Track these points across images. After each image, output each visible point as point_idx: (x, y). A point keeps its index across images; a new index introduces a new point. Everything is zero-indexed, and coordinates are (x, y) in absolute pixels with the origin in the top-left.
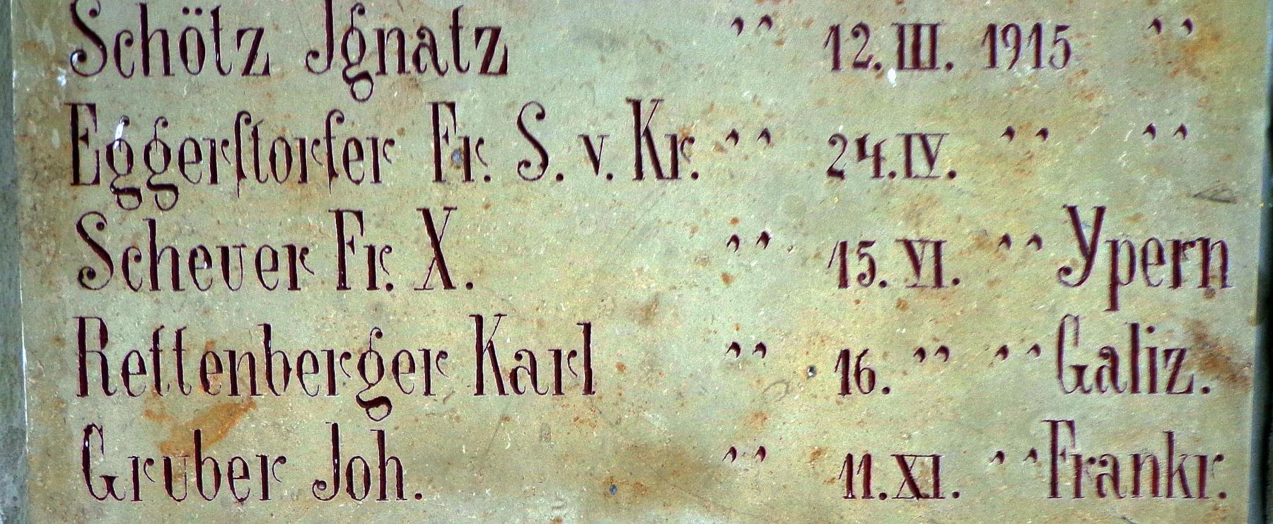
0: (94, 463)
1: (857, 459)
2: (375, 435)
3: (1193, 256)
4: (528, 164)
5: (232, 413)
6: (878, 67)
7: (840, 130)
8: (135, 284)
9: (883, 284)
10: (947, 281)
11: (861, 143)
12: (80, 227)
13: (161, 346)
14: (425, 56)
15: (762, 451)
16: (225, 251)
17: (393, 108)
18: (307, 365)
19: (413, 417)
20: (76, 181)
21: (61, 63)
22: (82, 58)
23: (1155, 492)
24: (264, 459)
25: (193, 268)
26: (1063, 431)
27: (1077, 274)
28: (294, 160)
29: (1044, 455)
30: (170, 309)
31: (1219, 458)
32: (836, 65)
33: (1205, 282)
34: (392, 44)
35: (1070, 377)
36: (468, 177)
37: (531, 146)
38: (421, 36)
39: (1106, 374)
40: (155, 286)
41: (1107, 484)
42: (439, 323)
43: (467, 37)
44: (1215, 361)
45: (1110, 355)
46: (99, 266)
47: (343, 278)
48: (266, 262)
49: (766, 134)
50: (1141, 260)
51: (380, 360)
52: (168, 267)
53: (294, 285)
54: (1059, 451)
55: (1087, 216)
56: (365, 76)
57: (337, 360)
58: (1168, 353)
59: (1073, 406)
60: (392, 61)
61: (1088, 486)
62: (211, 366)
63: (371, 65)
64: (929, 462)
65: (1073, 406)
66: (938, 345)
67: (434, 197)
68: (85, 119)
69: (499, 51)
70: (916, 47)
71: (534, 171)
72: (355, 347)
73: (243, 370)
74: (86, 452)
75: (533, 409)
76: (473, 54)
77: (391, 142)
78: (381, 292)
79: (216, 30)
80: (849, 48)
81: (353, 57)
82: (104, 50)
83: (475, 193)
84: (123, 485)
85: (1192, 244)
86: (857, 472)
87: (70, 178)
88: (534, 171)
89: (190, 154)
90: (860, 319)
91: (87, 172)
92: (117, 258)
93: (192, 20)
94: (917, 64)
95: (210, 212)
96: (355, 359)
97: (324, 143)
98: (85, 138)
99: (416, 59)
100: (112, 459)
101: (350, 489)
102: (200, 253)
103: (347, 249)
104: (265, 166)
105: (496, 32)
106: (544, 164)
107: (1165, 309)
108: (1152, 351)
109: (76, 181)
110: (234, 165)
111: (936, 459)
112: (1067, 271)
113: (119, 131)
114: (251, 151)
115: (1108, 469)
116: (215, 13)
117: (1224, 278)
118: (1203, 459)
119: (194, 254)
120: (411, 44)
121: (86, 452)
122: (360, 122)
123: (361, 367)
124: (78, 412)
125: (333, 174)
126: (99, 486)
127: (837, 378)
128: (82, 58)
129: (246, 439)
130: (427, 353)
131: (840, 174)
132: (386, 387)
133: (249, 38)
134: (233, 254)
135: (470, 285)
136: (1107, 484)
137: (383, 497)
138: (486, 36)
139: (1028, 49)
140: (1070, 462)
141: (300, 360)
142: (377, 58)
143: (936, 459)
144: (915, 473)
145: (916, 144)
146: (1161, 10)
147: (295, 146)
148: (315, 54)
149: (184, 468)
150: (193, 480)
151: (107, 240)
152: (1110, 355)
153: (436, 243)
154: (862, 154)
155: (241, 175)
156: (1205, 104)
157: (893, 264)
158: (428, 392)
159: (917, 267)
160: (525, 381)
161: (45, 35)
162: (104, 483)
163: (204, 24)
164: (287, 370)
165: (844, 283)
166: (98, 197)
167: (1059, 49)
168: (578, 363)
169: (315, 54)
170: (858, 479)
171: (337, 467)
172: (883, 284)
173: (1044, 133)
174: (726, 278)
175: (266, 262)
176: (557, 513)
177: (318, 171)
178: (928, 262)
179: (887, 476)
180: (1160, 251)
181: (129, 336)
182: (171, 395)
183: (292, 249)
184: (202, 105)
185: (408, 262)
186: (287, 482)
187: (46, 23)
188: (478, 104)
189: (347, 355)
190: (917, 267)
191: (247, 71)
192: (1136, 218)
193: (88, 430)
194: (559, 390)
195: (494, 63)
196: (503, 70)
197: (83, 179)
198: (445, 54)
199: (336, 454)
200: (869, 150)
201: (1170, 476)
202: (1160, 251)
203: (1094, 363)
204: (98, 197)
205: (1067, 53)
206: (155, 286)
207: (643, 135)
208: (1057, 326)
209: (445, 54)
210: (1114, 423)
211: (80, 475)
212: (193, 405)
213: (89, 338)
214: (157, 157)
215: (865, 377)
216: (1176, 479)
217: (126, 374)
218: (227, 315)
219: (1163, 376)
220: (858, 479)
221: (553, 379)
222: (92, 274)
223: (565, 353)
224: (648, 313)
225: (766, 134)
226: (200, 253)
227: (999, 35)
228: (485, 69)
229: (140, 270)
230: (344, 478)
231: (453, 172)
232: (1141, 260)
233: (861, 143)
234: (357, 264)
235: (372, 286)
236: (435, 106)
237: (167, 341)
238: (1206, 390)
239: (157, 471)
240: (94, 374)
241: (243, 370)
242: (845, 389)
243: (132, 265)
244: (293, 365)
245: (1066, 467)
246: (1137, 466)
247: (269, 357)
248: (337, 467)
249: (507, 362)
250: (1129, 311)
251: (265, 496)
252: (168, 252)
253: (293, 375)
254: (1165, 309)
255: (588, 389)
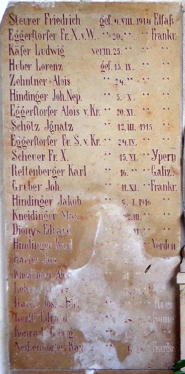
0: (14, 185)
1: (124, 185)
2: (55, 182)
3: (171, 156)
4: (76, 143)
5: (34, 178)
6: (125, 130)
7: (120, 139)
8: (20, 160)
9: (127, 160)
10: (136, 160)
11: (123, 140)
12: (13, 152)
13: (24, 169)
14: (61, 128)
15: (110, 184)
16: (33, 155)
17: (57, 135)
18: (45, 172)
19: (60, 180)
20: (12, 145)
21: (10, 129)
22: (13, 128)
23: (167, 190)
24: (39, 185)
25: (28, 158)
26: (153, 181)
27: (154, 159)
28: (43, 142)
29: (151, 185)
30: (25, 163)
31: (176, 185)
32: (119, 130)
33: (172, 160)
34: (57, 126)
35: (154, 174)
36: (68, 145)
37: (76, 141)
38: (61, 125)
39: (159, 173)
40: (23, 160)
41: (160, 189)
42: (63, 165)
43: (67, 126)
44: (175, 172)
45: (159, 170)
46: (15, 157)
47: (50, 159)
48: (39, 157)
49: (110, 139)
50: (163, 157)
51: (55, 171)
52: (24, 157)
53: (43, 160)
54: (153, 184)
55: (155, 151)
56: (53, 131)
57: (49, 171)
58: (168, 170)
59: (154, 178)
60: (57, 129)
61: (157, 189)
62: (31, 172)
63: (54, 129)
64: (134, 186)
65: (154, 178)
66: (135, 169)
67: (63, 148)
68: (13, 137)
69: (72, 127)
70: (130, 127)
71: (77, 144)
72: (52, 169)
73: (35, 172)
74: (13, 184)
75: (77, 178)
76: (68, 128)
77: (57, 140)
78: (55, 161)
79: (32, 124)
80: (121, 127)
81: (51, 128)
82: (16, 127)
83: (69, 147)
84: (18, 189)
85: (170, 155)
86: (124, 187)
87: (11, 145)
88: (77, 144)
89: (28, 142)
90: (124, 165)
91: (14, 144)
92: (18, 156)
93: (29, 123)
94: (131, 130)
95: (30, 150)
96: (52, 171)
97: (47, 140)
98: (14, 139)
99: (60, 129)
100: (17, 185)
101: (51, 189)
102: (29, 155)
103: (51, 155)
104: (39, 143)
105: (71, 125)
106: (78, 143)
107: (167, 164)
108: (165, 170)
109: (12, 145)
110: (34, 143)
111: (135, 185)
112: (153, 159)
113: (18, 138)
114: (37, 141)
115: (160, 187)
116: (32, 122)
117: (175, 160)
118: (173, 185)
119: (29, 156)
120: (60, 126)
121: (13, 184)
122: (52, 137)
123: (53, 172)
124: (12, 178)
125: (49, 145)
126: (15, 189)
127: (120, 174)
128: (13, 128)
129: (35, 182)
130: (62, 170)
131: (120, 145)
132: (56, 175)
133: (36, 126)
134: (34, 156)
135: (68, 160)
136: (160, 189)
137: (56, 190)
138: (70, 125)
139: (146, 128)
140: (154, 185)
141: (44, 171)
142: (55, 128)
143: (135, 185)
144: (132, 187)
145: (131, 140)
146: (164, 122)
147: (43, 141)
148: (46, 128)
149: (27, 186)
150: (28, 188)
151: (16, 154)
152: (159, 170)
153: (63, 154)
154: (123, 142)
155: (35, 145)
156: (171, 135)
157: (128, 157)
158: (62, 175)
159: (132, 158)
160: (76, 174)
161: (7, 125)
162: (15, 188)
163: (30, 124)
164: (42, 172)
165: (121, 160)
166: (15, 148)
167: (151, 127)
168: (84, 171)
169: (46, 128)
170: (124, 188)
171: (49, 186)
172: (127, 160)
173: (149, 139)
174: (105, 159)
175: (39, 157)
176: (81, 193)
177: (46, 144)
178: (133, 157)
179: (128, 188)
180: (166, 156)
181: (19, 167)
182: (25, 176)
183: (43, 155)
184: (30, 135)
185: (59, 157)
186: (42, 188)
187: (8, 123)
188: (69, 135)
189: (51, 170)
190: (132, 158)
191: (36, 130)
192: (162, 151)
193: (13, 181)
194: (81, 175)
195: (71, 129)
196: (72, 130)
197: (13, 145)
198: (64, 128)
199: (49, 184)
200: (124, 141)
201: (169, 188)
202: (166, 156)
203: (157, 172)
204: (15, 148)
205: (152, 128)
206: (23, 160)
207: (92, 139)
208: (152, 166)
209: (64, 128)
210: (160, 180)
211: (12, 187)
212: (28, 177)
213: (14, 167)
214: (23, 142)
215: (125, 173)
216: (170, 188)
217: (19, 173)
218: (33, 164)
219: (167, 173)
220: (124, 188)
221: (80, 174)
222: (14, 159)
223: (82, 170)
224: (93, 164)
225: (110, 139)
226: (29, 155)
227: (142, 125)
228: (70, 130)
229: (21, 158)
230: (50, 188)
231: (65, 144)
232: (163, 157)
233: (123, 140)
234: (52, 157)
235: (54, 160)
236: (63, 135)
237: (25, 168)
238: (173, 175)
239: (23, 187)
240: (14, 173)
241: (35, 172)
242: (122, 175)
243: (20, 157)
244: (43, 171)
245: (154, 187)
246: (164, 187)
247: (39, 170)
248: (49, 186)
249: (73, 171)
250: (162, 164)
251: (39, 190)
252: (25, 155)
253: (43, 173)
254: (167, 164)
255: (85, 175)
